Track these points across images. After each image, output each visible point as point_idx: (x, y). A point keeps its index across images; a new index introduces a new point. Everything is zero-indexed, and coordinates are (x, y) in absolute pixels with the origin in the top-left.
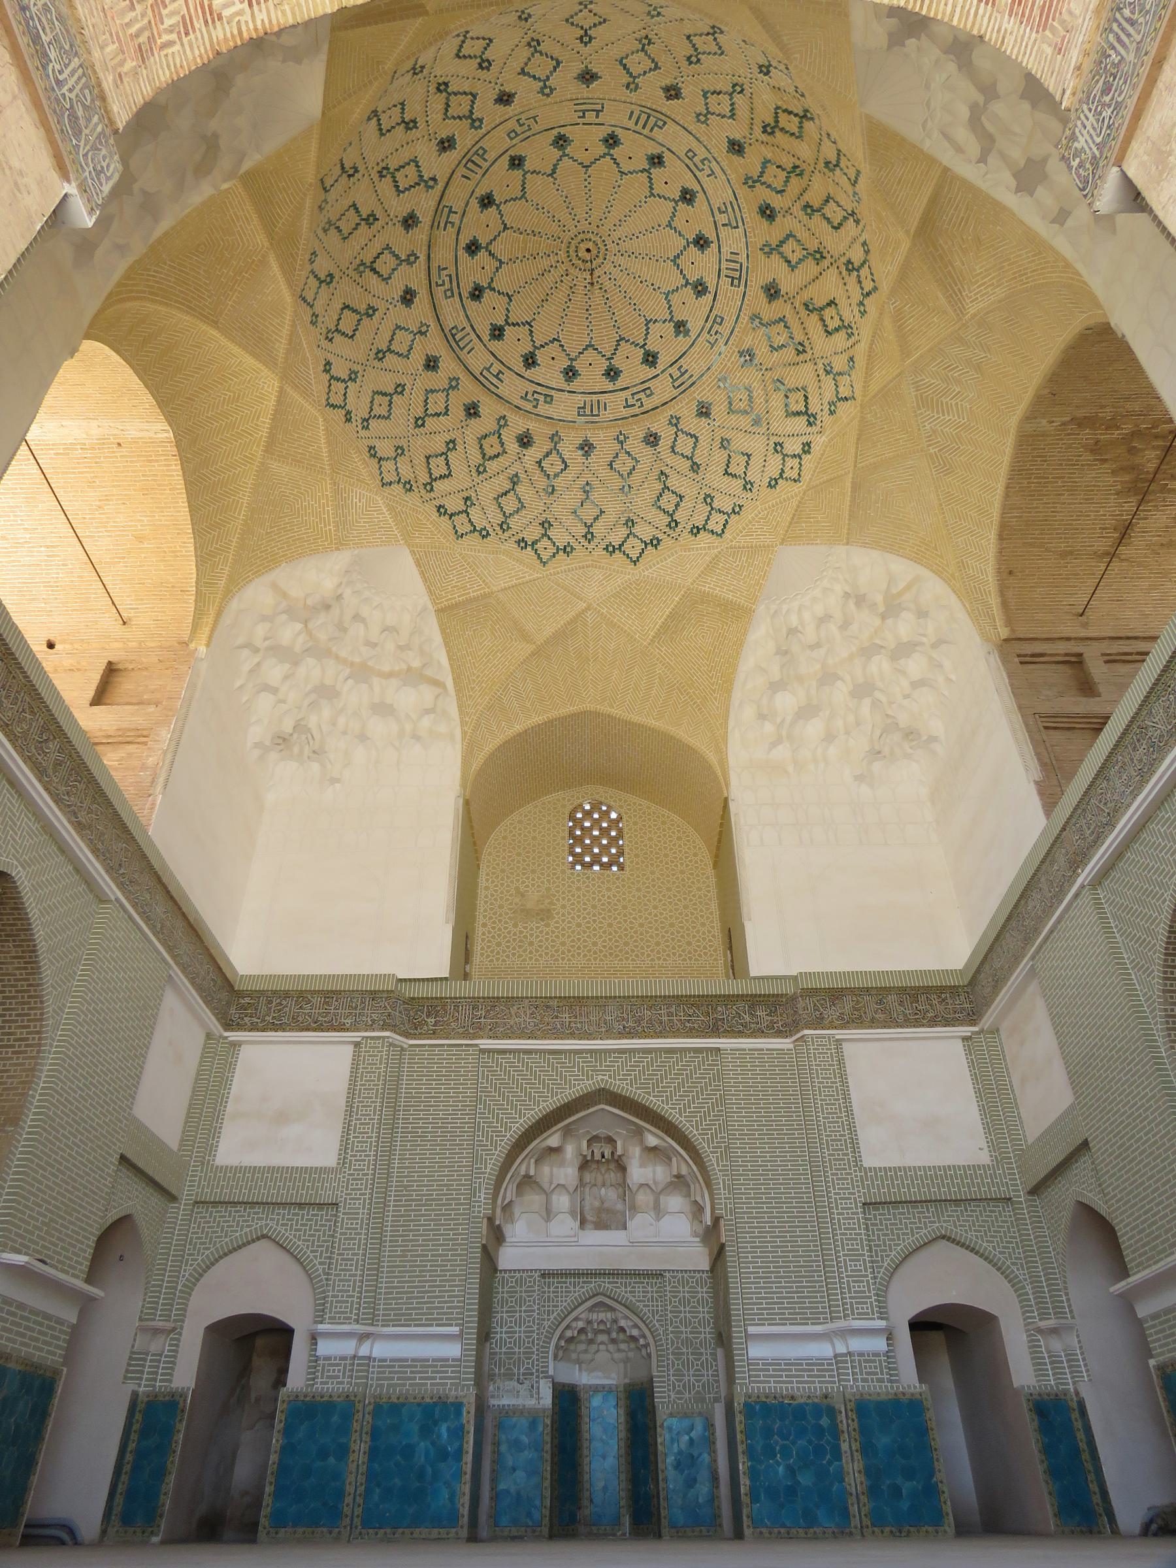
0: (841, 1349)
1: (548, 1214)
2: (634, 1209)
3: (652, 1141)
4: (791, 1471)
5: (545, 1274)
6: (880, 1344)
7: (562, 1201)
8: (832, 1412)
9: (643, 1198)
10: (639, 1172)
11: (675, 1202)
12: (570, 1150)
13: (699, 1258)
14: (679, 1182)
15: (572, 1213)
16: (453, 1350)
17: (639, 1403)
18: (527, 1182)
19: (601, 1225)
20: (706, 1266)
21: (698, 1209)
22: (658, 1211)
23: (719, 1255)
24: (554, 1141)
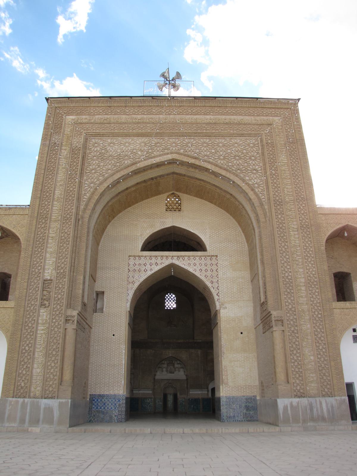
0: (201, 392)
1: (162, 371)
2: (175, 370)
3: (178, 362)
4: (194, 406)
5: (162, 379)
6: (207, 392)
7: (165, 369)
8: (200, 400)
9: (177, 369)
10: (176, 366)
11: (181, 370)
12: (166, 362)
13: (184, 377)
14: (182, 368)
15: (166, 371)
16: (151, 392)
17: (175, 396)
18: (159, 367)
19: (171, 372)
20: (186, 378)
21: (185, 372)
22: (179, 371)
23: (187, 379)
24: (163, 362)
